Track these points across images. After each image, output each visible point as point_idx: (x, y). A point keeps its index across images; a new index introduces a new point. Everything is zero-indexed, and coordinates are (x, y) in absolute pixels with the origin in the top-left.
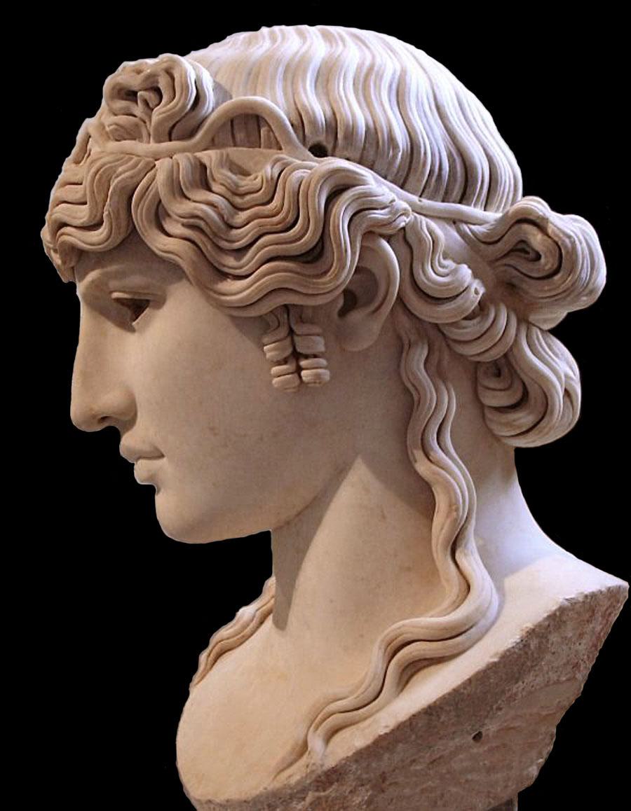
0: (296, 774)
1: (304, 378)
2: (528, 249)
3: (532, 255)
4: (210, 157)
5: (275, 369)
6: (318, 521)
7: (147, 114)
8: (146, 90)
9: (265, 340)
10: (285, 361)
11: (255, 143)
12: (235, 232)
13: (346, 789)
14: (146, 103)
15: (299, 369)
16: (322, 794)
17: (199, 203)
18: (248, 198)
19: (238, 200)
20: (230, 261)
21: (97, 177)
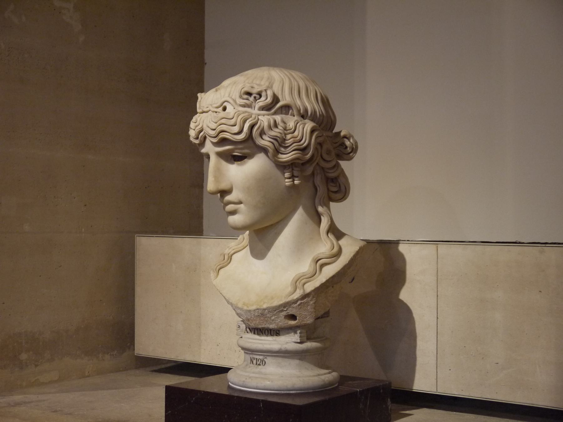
0: (296, 296)
1: (295, 183)
2: (344, 145)
3: (345, 147)
4: (278, 118)
5: (287, 180)
6: (286, 225)
7: (254, 100)
8: (256, 94)
9: (285, 171)
10: (289, 178)
11: (287, 113)
12: (286, 142)
13: (309, 299)
14: (255, 97)
15: (293, 181)
16: (302, 301)
17: (275, 132)
18: (288, 131)
19: (286, 132)
20: (282, 149)
21: (242, 120)
